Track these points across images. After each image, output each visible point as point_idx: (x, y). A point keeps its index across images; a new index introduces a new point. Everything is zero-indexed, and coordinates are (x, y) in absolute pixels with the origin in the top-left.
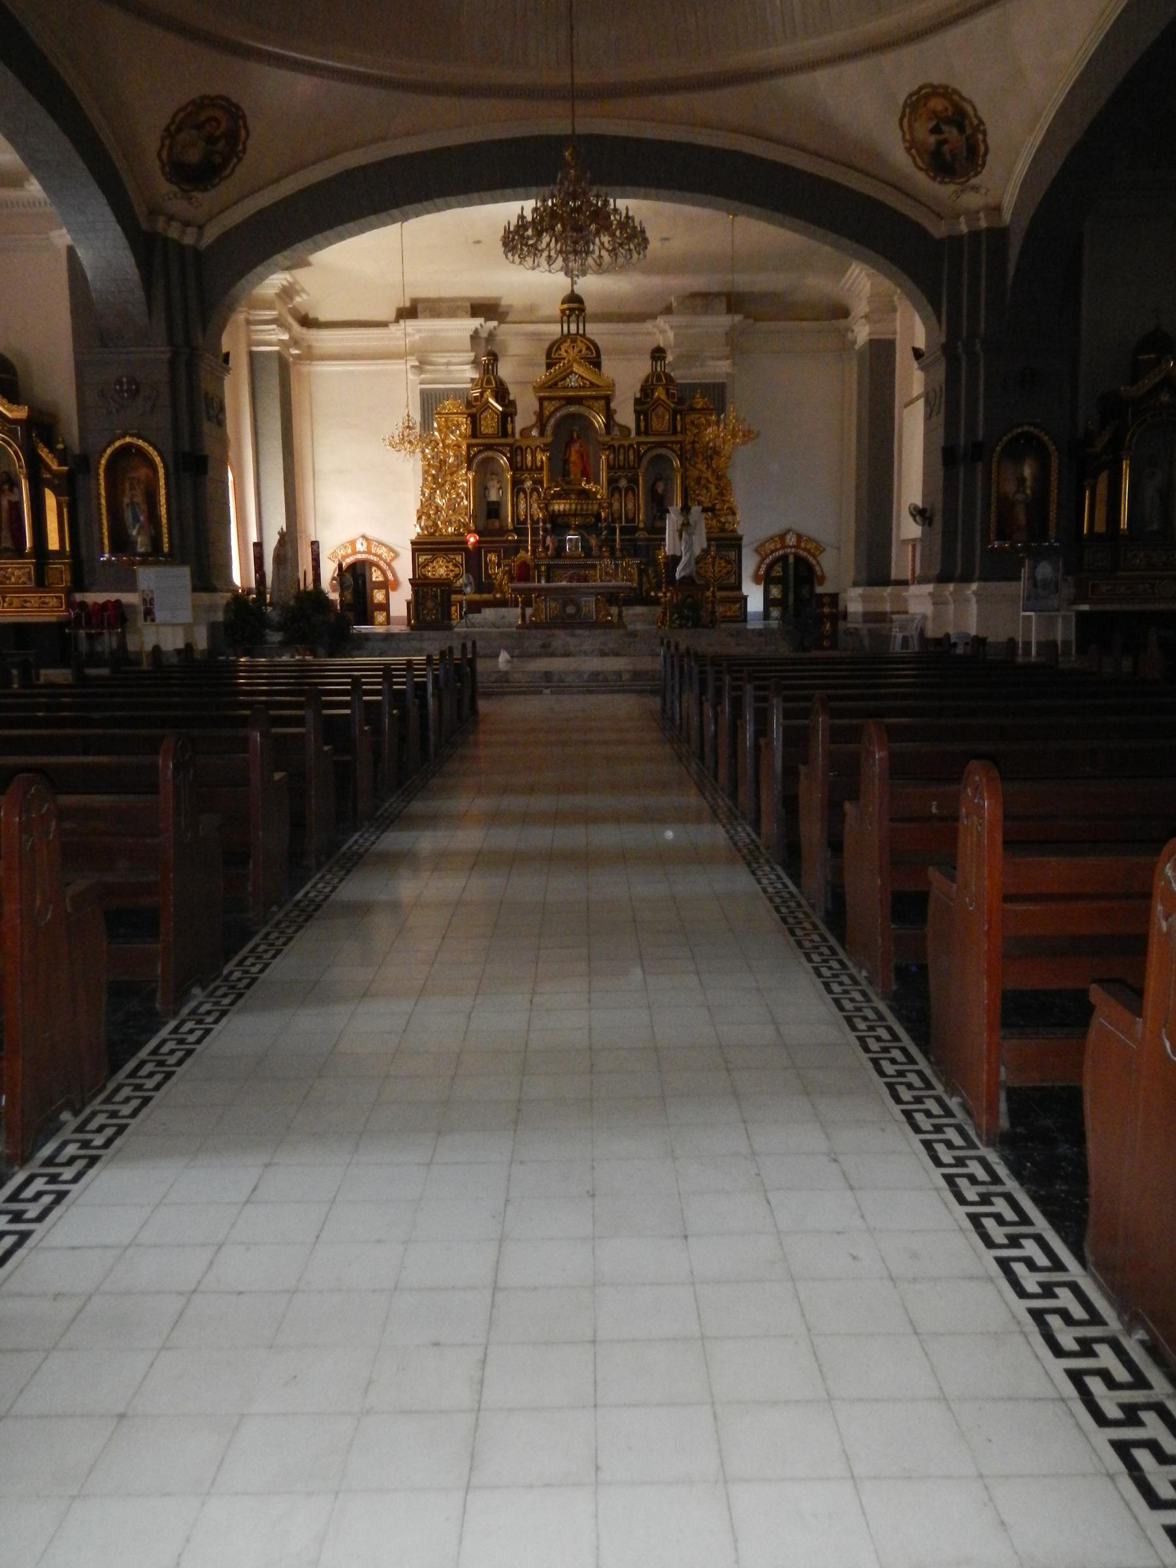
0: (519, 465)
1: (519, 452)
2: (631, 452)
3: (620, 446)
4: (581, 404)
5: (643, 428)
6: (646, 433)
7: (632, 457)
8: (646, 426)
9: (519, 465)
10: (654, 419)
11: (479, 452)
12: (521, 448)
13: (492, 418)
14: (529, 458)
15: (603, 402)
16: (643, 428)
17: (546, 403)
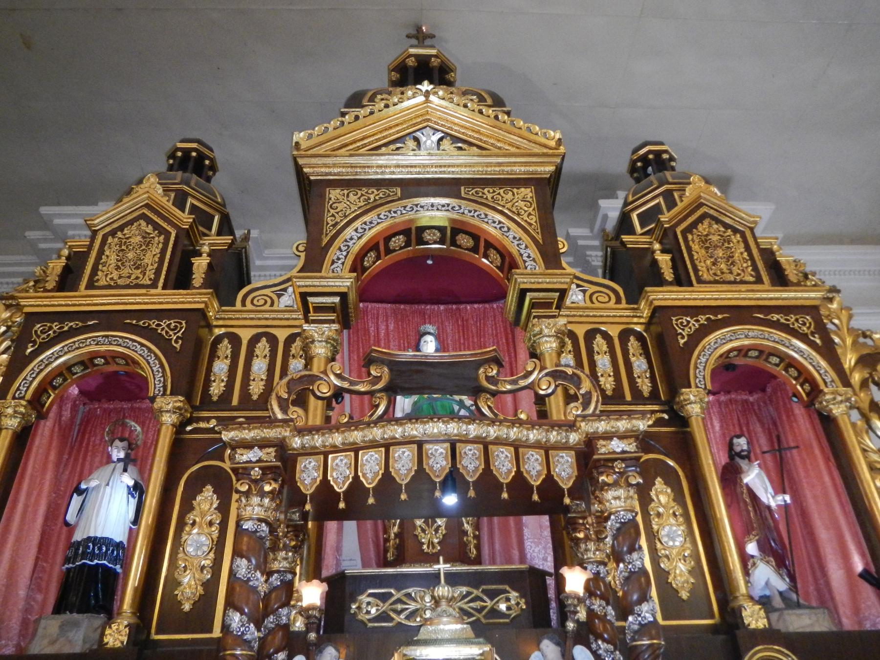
0: (216, 389)
1: (225, 348)
2: (633, 344)
3: (590, 335)
4: (458, 196)
5: (669, 275)
6: (682, 279)
7: (640, 364)
8: (678, 264)
9: (216, 389)
10: (695, 247)
11: (60, 337)
12: (235, 340)
13: (147, 241)
14: (259, 366)
15: (527, 192)
16: (669, 275)
17: (334, 194)
